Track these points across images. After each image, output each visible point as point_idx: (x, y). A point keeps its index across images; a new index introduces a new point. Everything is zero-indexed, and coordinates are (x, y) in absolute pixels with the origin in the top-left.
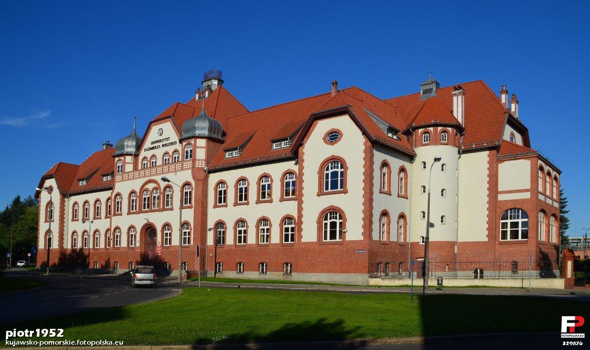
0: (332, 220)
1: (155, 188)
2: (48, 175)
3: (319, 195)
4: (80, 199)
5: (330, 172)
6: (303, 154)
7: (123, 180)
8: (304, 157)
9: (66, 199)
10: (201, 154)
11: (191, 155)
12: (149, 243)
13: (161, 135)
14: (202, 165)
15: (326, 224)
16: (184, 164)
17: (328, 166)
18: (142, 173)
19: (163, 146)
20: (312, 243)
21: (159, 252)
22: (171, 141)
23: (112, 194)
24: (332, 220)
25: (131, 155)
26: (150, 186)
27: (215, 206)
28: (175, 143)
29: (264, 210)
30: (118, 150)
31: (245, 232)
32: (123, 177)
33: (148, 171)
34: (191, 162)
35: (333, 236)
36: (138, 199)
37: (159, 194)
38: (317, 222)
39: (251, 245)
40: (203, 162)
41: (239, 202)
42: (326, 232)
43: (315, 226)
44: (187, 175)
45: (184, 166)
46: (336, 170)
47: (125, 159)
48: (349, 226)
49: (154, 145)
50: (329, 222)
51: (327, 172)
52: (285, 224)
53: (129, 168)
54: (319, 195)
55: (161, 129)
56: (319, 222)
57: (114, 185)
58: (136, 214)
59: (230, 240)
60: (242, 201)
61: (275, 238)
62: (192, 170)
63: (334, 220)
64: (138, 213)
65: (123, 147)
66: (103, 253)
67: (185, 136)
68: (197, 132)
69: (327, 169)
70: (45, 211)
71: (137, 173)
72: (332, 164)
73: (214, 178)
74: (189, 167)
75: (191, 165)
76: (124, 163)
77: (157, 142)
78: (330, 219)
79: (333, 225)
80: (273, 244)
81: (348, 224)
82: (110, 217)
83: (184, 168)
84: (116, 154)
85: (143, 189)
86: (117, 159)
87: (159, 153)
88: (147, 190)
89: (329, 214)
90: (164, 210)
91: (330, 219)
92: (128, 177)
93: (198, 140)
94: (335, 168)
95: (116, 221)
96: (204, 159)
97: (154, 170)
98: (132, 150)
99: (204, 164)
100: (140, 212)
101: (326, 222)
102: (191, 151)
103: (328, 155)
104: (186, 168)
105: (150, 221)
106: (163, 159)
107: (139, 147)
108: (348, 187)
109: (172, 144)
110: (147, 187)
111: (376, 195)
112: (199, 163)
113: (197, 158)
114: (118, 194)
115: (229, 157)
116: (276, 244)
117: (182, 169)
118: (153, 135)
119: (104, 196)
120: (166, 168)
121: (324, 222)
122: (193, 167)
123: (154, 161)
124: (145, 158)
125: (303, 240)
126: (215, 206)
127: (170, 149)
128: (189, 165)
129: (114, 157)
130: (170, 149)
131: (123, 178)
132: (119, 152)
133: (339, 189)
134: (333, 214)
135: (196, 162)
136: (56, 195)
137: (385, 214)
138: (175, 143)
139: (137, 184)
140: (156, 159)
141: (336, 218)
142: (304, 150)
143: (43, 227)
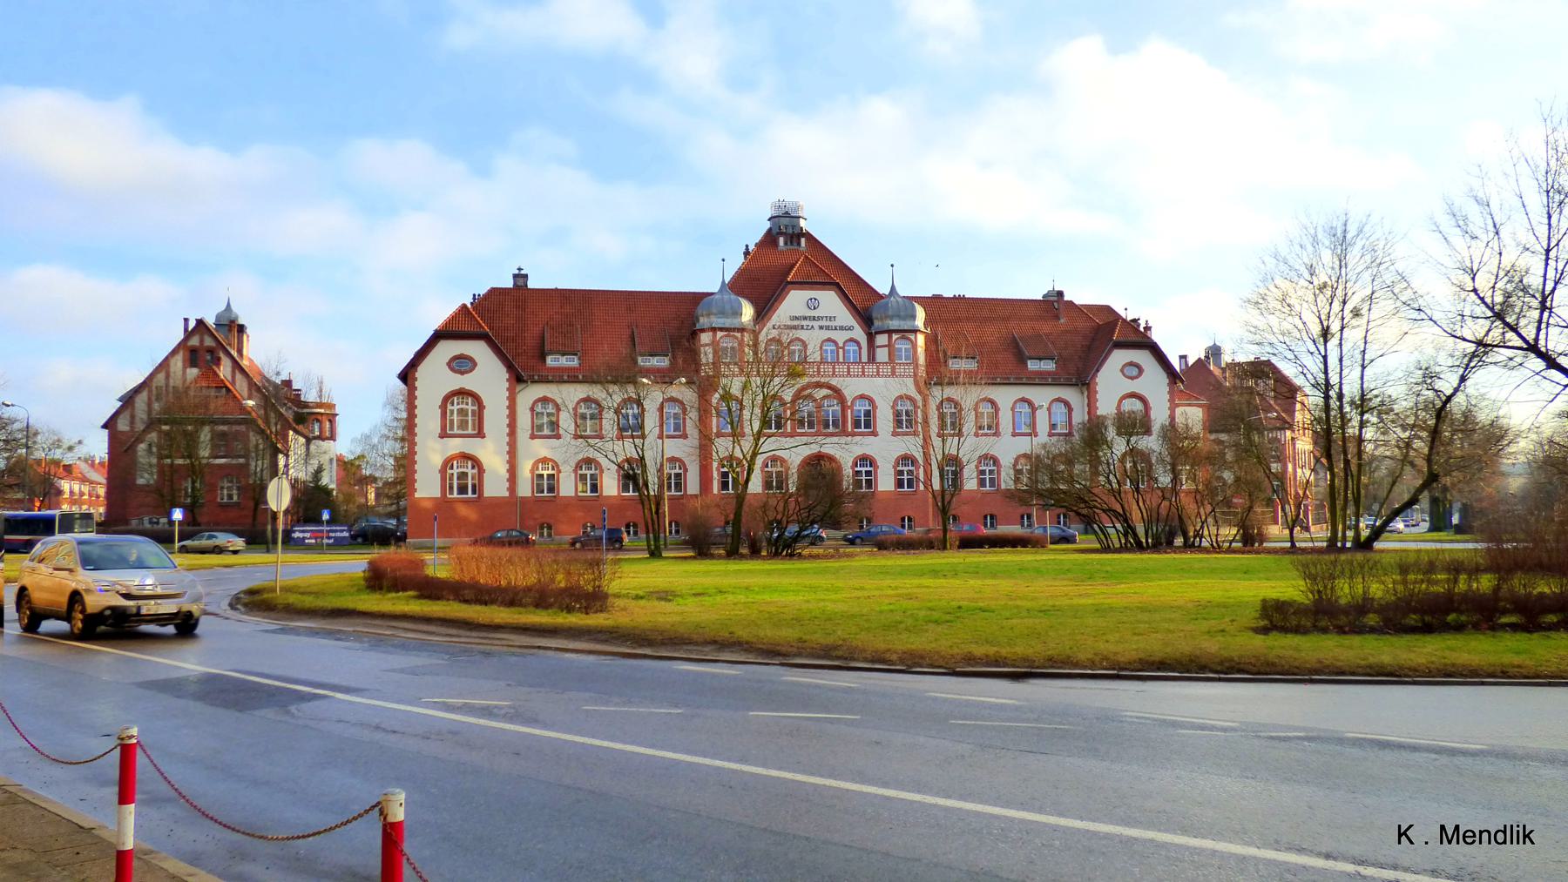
9: (519, 387)
13: (815, 308)
19: (821, 328)
29: (987, 445)
55: (815, 299)
77: (805, 318)
88: (810, 396)
109: (842, 328)
117: (893, 374)
130: (841, 337)
138: (850, 328)
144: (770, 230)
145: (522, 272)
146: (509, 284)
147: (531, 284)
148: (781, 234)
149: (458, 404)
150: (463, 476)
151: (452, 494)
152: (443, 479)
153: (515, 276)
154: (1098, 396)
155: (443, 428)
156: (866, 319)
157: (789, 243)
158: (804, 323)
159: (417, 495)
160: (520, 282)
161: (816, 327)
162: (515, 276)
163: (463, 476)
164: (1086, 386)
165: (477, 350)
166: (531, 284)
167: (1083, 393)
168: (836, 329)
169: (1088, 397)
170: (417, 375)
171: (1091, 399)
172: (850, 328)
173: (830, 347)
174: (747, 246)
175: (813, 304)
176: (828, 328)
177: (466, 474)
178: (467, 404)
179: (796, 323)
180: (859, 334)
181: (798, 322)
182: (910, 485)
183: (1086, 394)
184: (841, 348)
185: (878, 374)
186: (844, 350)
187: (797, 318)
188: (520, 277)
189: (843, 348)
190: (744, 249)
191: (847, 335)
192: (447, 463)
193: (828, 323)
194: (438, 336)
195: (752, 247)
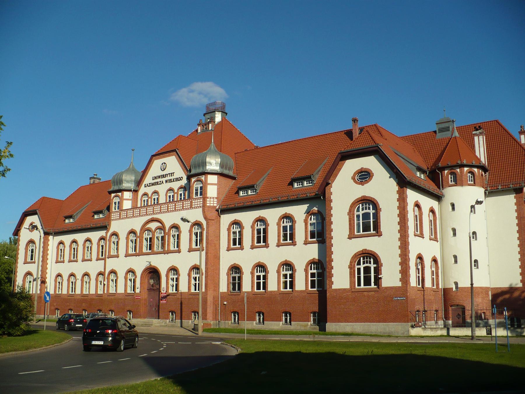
0: (366, 265)
1: (158, 228)
2: (31, 211)
3: (350, 238)
4: (67, 239)
5: (361, 213)
7: (120, 218)
10: (212, 191)
11: (203, 192)
12: (150, 289)
13: (164, 170)
14: (213, 204)
15: (359, 269)
16: (194, 201)
17: (359, 207)
18: (143, 210)
19: (166, 181)
20: (345, 289)
22: (176, 176)
23: (106, 233)
24: (366, 265)
25: (129, 190)
26: (153, 226)
27: (229, 249)
28: (180, 179)
30: (114, 185)
31: (265, 277)
32: (120, 214)
33: (150, 210)
34: (201, 200)
35: (367, 282)
36: (138, 239)
37: (163, 235)
38: (349, 267)
39: (271, 292)
40: (215, 200)
41: (256, 244)
42: (359, 278)
43: (347, 272)
44: (196, 215)
45: (193, 204)
46: (367, 211)
47: (122, 195)
48: (384, 270)
49: (158, 180)
50: (362, 267)
51: (358, 213)
52: (311, 269)
53: (127, 205)
54: (350, 238)
55: (165, 163)
56: (351, 267)
57: (109, 224)
58: (136, 256)
59: (247, 286)
60: (260, 243)
61: (300, 284)
62: (203, 208)
63: (368, 265)
64: (139, 256)
65: (120, 182)
66: (94, 299)
67: (193, 172)
68: (209, 168)
69: (358, 210)
70: (24, 251)
71: (137, 211)
72: (362, 205)
73: (227, 219)
74: (199, 205)
75: (201, 203)
76: (122, 199)
77: (159, 177)
78: (364, 263)
79: (367, 270)
80: (298, 291)
81: (383, 269)
82: (104, 259)
83: (193, 206)
84: (111, 189)
85: (144, 229)
86: (113, 195)
87: (162, 189)
88: (149, 230)
89: (362, 258)
90: (169, 252)
91: (364, 263)
92: (127, 215)
93: (209, 176)
94: (366, 209)
95: (111, 264)
96: (216, 197)
97: (157, 208)
98: (132, 186)
99: (216, 202)
100: (141, 254)
101: (359, 267)
102: (201, 188)
103: (359, 195)
104: (196, 206)
105: (153, 264)
106: (166, 195)
107: (139, 183)
108: (383, 228)
109: (178, 179)
110: (149, 226)
111: (412, 240)
112: (210, 201)
113: (209, 195)
114: (115, 234)
115: (244, 195)
116: (301, 291)
117: (191, 207)
118: (155, 169)
119: (95, 236)
120: (171, 206)
121: (357, 267)
122: (204, 206)
123: (156, 197)
124: (145, 194)
125: (334, 287)
126: (229, 249)
128: (199, 203)
129: (110, 193)
131: (120, 216)
132: (116, 188)
133: (372, 232)
134: (367, 259)
135: (208, 200)
136: (37, 235)
137: (420, 257)
138: (180, 179)
139: (137, 224)
140: (158, 195)
141: (370, 263)
142: (332, 190)
143: (21, 269)
158: (158, 180)
161: (164, 182)
168: (174, 181)
176: (170, 181)
185: (183, 209)
187: (156, 178)
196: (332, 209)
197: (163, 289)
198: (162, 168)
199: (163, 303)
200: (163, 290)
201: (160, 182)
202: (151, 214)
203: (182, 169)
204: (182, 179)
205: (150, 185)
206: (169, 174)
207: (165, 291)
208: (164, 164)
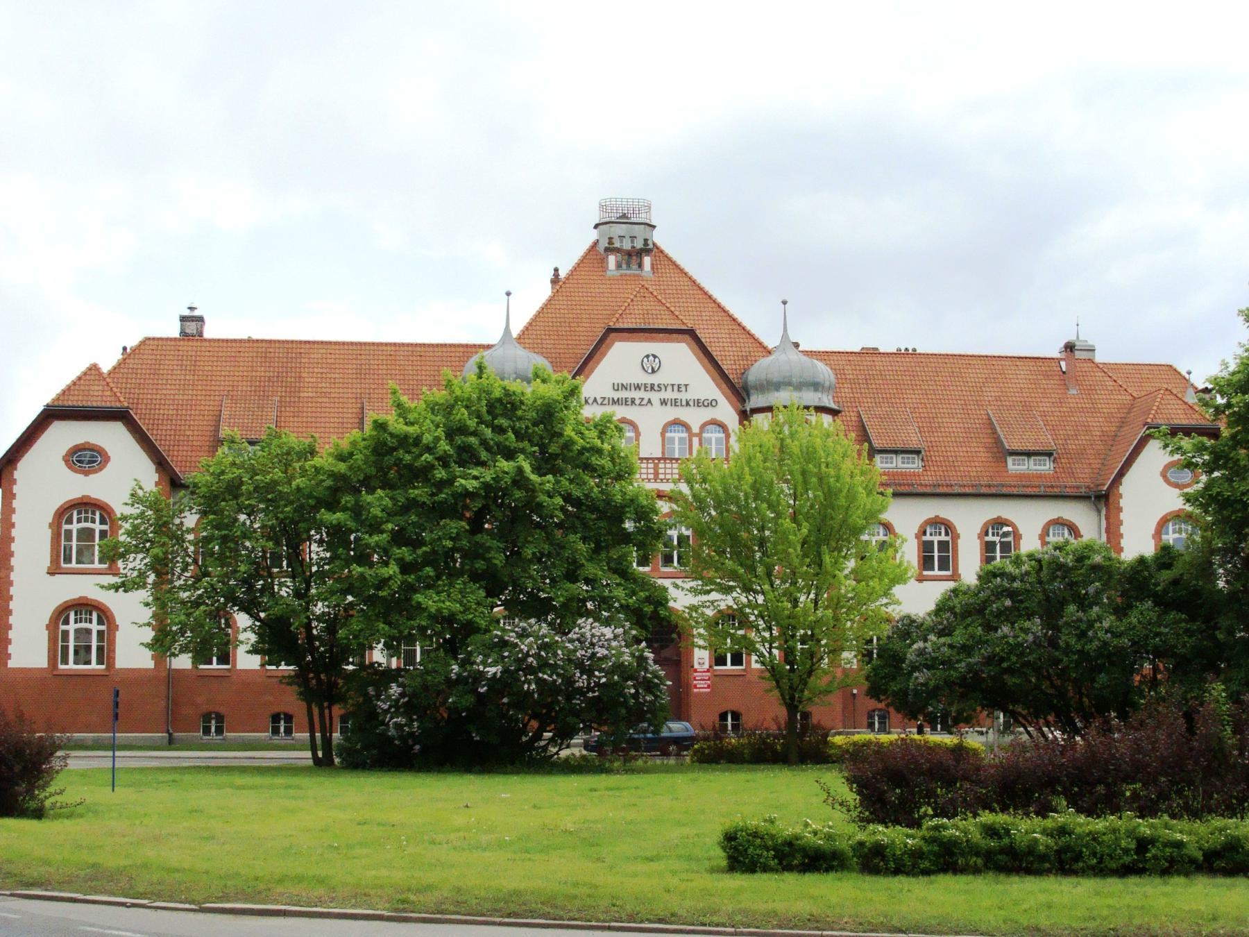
6: (1121, 496)
8: (1122, 503)
13: (653, 371)
19: (664, 402)
21: (701, 684)
22: (691, 395)
55: (655, 357)
77: (638, 387)
109: (698, 403)
127: (696, 418)
130: (696, 418)
138: (712, 404)
144: (596, 243)
145: (196, 313)
146: (175, 332)
147: (211, 331)
148: (609, 250)
149: (79, 521)
150: (84, 634)
151: (67, 663)
152: (53, 641)
153: (184, 319)
154: (1122, 516)
155: (55, 560)
156: (738, 391)
157: (624, 266)
158: (637, 395)
159: (12, 664)
160: (191, 328)
161: (656, 401)
162: (184, 319)
163: (84, 634)
164: (1103, 501)
165: (112, 437)
166: (211, 331)
167: (1099, 511)
168: (688, 404)
169: (1107, 518)
170: (17, 475)
171: (1112, 520)
172: (712, 404)
173: (677, 435)
174: (556, 270)
175: (652, 365)
176: (675, 403)
177: (89, 631)
178: (93, 521)
179: (616, 395)
180: (727, 412)
181: (625, 393)
182: (737, 660)
183: (1104, 512)
184: (696, 435)
186: (700, 440)
187: (624, 387)
188: (192, 321)
189: (699, 435)
190: (550, 274)
191: (706, 414)
192: (61, 614)
193: (676, 396)
194: (50, 416)
195: (563, 274)
196: (1122, 524)
197: (701, 661)
198: (648, 368)
199: (701, 694)
200: (699, 663)
201: (643, 399)
202: (649, 480)
203: (713, 380)
204: (714, 404)
205: (606, 402)
206: (673, 385)
207: (706, 666)
208: (651, 358)
